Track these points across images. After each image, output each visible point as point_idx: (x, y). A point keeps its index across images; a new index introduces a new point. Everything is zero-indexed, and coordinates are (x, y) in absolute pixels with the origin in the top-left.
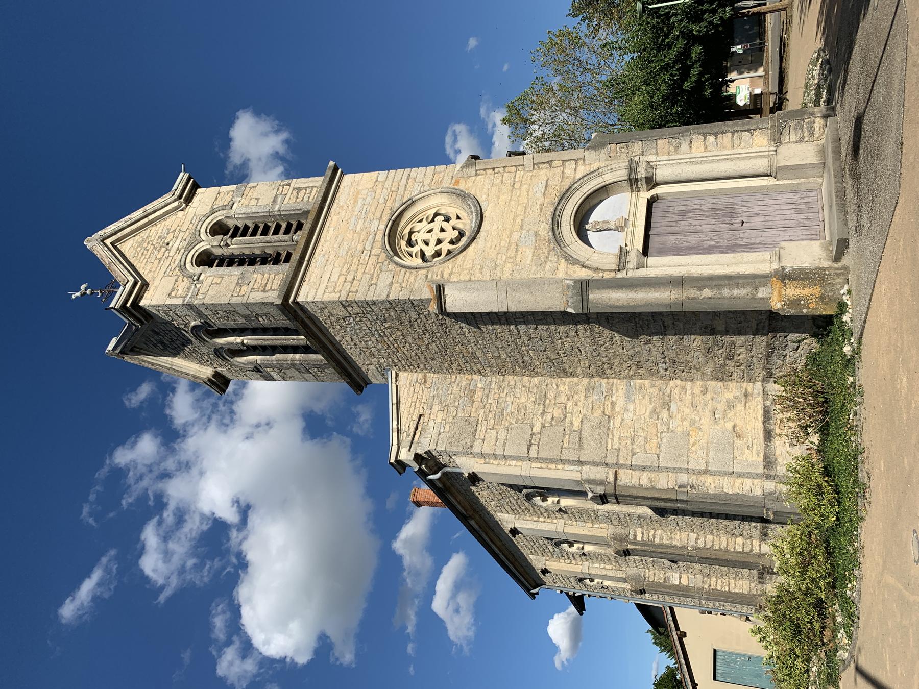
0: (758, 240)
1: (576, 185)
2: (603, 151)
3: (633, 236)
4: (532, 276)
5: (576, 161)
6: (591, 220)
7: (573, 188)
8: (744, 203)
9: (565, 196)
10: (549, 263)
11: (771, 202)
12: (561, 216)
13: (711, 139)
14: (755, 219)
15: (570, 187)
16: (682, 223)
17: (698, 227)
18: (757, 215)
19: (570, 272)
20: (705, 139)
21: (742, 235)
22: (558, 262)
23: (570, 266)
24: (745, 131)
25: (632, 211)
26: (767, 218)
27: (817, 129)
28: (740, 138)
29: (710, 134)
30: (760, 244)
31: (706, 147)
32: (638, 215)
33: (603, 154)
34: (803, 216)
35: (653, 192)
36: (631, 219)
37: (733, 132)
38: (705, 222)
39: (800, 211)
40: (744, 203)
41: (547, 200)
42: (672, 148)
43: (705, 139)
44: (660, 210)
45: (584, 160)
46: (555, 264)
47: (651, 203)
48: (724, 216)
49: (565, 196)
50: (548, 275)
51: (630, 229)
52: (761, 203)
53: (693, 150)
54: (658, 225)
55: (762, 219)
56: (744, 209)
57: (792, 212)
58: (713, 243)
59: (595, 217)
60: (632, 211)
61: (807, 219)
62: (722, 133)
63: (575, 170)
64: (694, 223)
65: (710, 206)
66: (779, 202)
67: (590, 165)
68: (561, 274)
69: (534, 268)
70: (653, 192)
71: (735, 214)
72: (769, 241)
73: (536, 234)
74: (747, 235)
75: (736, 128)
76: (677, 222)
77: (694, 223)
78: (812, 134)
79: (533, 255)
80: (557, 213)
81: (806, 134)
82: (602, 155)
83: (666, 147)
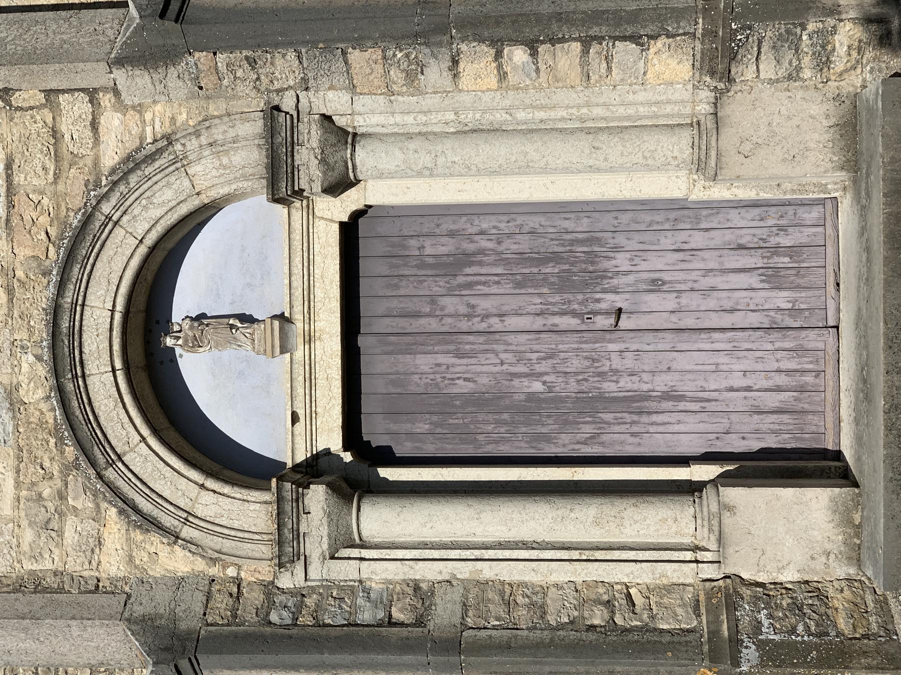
0: (661, 383)
1: (106, 208)
2: (173, 72)
3: (310, 380)
4: (29, 566)
5: (92, 94)
6: (177, 316)
7: (100, 218)
8: (621, 239)
9: (78, 245)
10: (71, 523)
11: (697, 240)
12: (77, 333)
13: (518, 55)
14: (653, 301)
15: (88, 219)
16: (451, 304)
17: (494, 321)
18: (656, 285)
19: (141, 557)
20: (498, 55)
21: (616, 362)
22: (97, 517)
23: (138, 536)
24: (624, 38)
25: (297, 283)
26: (684, 300)
27: (842, 50)
28: (608, 60)
29: (515, 42)
30: (667, 396)
31: (502, 76)
32: (319, 293)
33: (175, 79)
34: (781, 299)
35: (351, 201)
36: (298, 317)
37: (586, 43)
38: (512, 303)
39: (774, 278)
40: (621, 239)
41: (23, 252)
42: (395, 74)
43: (498, 55)
44: (380, 248)
45: (116, 92)
46: (90, 526)
47: (349, 232)
48: (564, 284)
49: (78, 245)
50: (75, 565)
51: (299, 354)
52: (667, 241)
53: (465, 81)
54: (381, 307)
55: (669, 302)
56: (621, 261)
57: (753, 280)
58: (537, 386)
59: (188, 297)
60: (297, 283)
61: (794, 312)
62: (553, 41)
63: (94, 126)
64: (484, 305)
65: (524, 244)
66: (718, 238)
67: (139, 109)
68: (112, 565)
69: (28, 535)
70: (351, 201)
71: (597, 279)
72: (687, 387)
73: (15, 404)
74: (629, 362)
75: (595, 31)
76: (433, 300)
77: (484, 305)
78: (823, 61)
79: (18, 485)
80: (65, 324)
81: (806, 61)
82: (172, 81)
83: (379, 68)
